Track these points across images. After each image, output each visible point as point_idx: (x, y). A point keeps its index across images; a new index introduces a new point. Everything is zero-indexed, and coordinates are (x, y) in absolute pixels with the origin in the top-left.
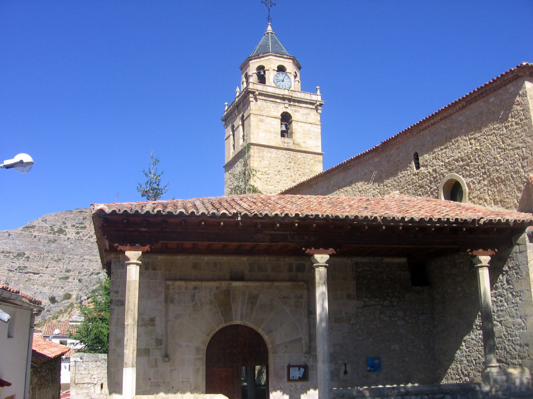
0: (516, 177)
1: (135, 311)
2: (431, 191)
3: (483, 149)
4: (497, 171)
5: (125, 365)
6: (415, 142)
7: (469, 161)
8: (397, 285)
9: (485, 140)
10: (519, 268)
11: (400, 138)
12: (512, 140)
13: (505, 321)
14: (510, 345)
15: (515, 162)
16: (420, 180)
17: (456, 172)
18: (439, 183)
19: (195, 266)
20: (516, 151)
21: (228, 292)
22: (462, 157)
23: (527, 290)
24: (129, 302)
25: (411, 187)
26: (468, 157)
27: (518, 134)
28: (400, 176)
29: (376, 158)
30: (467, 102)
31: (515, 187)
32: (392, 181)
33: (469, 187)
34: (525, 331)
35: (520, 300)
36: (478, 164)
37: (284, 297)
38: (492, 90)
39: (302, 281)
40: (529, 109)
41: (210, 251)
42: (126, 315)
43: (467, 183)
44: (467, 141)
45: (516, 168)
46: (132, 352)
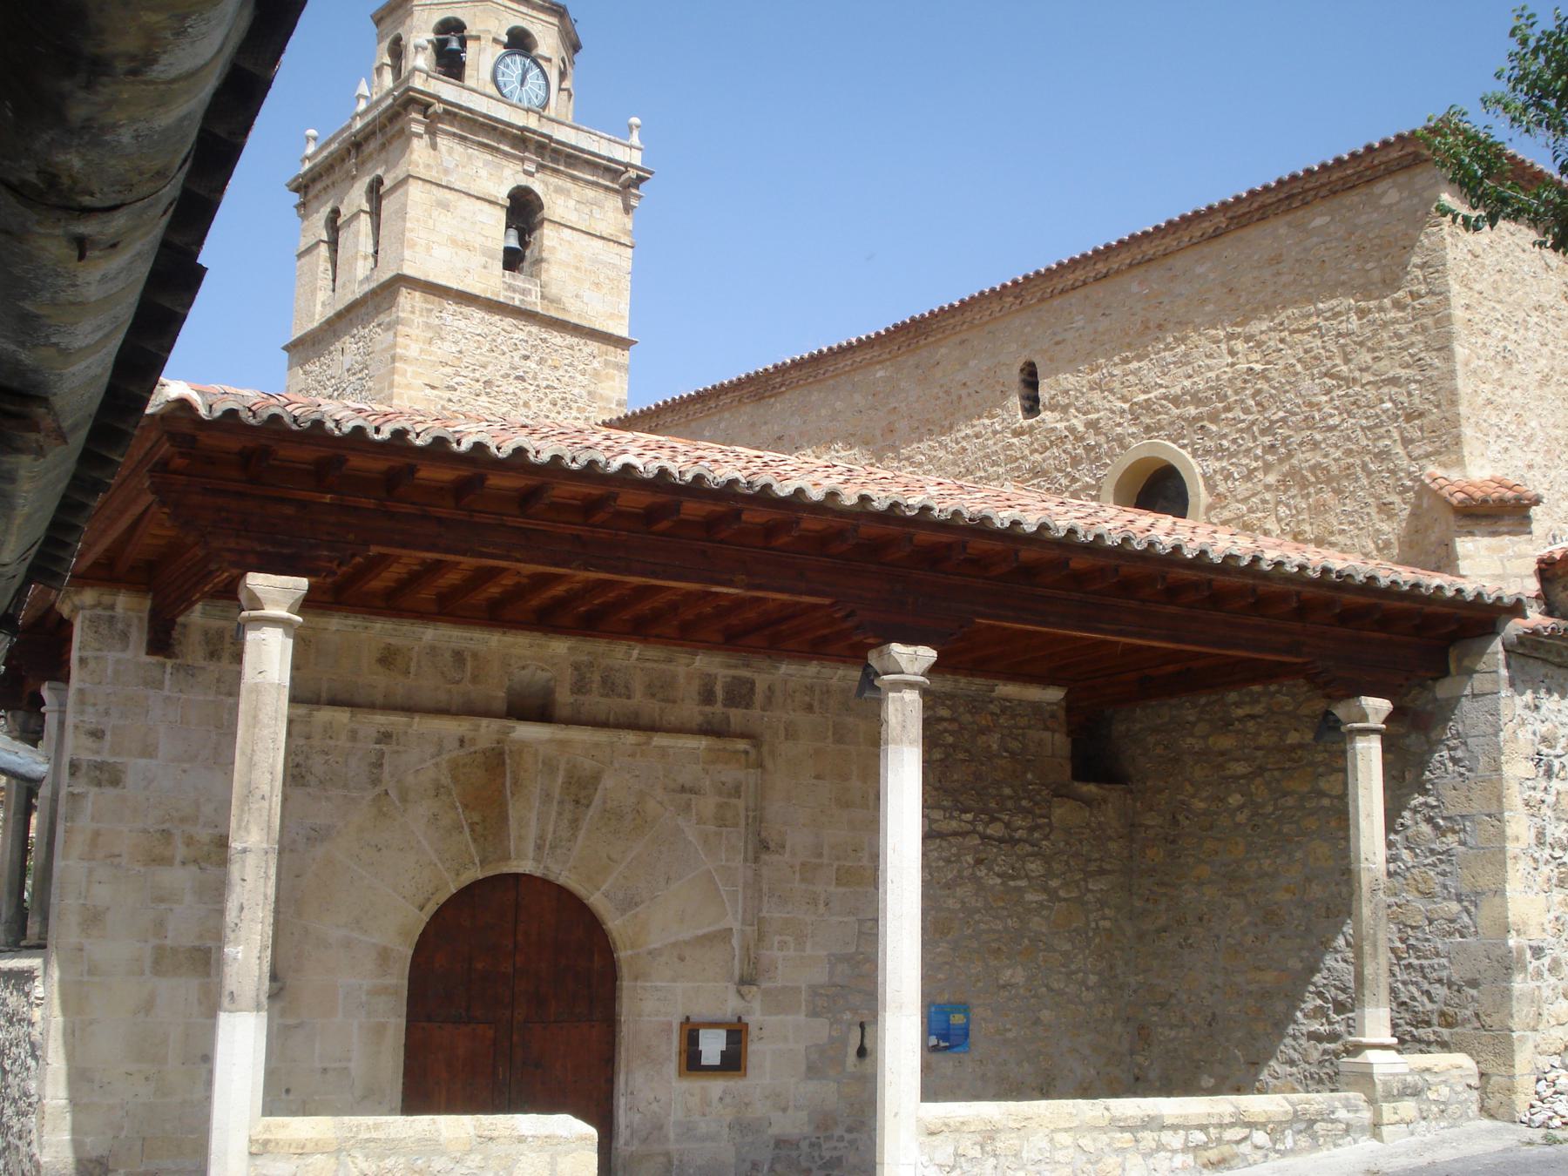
0: (1380, 472)
1: (274, 799)
2: (1071, 489)
3: (1273, 374)
4: (1316, 445)
5: (226, 1001)
6: (1028, 329)
7: (1220, 405)
8: (1029, 776)
9: (1281, 346)
10: (1465, 744)
11: (976, 309)
12: (1377, 354)
13: (1399, 906)
14: (1413, 983)
15: (1381, 424)
16: (1036, 451)
17: (1169, 437)
18: (1106, 465)
19: (388, 658)
20: (1385, 390)
21: (496, 760)
22: (1198, 391)
23: (1490, 816)
24: (251, 765)
25: (1001, 470)
26: (1217, 394)
27: (1399, 337)
28: (963, 434)
29: (878, 367)
30: (1232, 218)
31: (1370, 500)
32: (932, 448)
33: (1211, 486)
34: (1470, 939)
35: (1462, 843)
36: (1251, 417)
37: (683, 789)
38: (1324, 192)
39: (743, 736)
40: (1444, 265)
41: (449, 609)
42: (234, 810)
43: (1204, 475)
44: (1220, 341)
45: (1381, 444)
46: (256, 953)
